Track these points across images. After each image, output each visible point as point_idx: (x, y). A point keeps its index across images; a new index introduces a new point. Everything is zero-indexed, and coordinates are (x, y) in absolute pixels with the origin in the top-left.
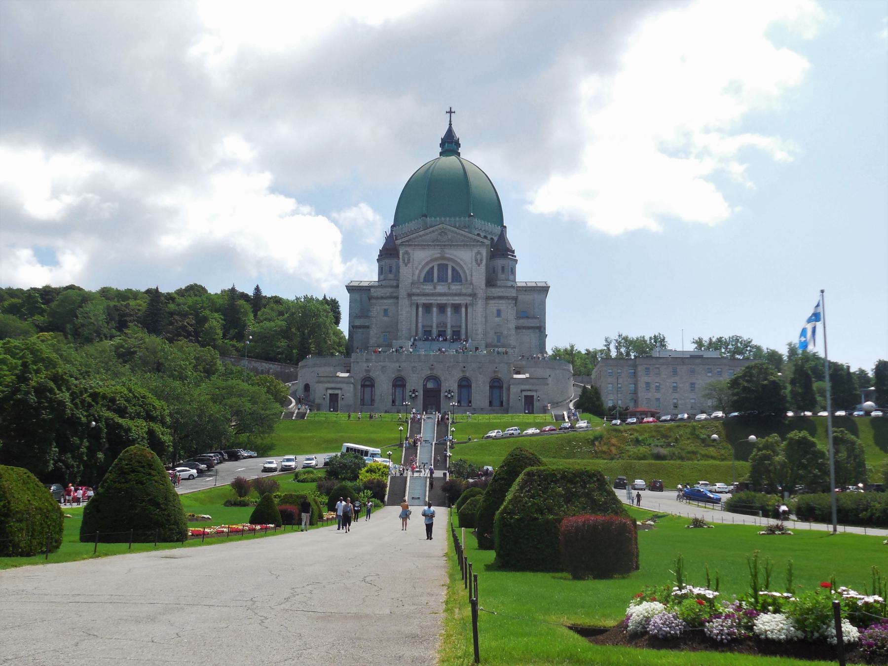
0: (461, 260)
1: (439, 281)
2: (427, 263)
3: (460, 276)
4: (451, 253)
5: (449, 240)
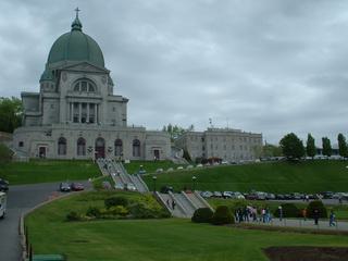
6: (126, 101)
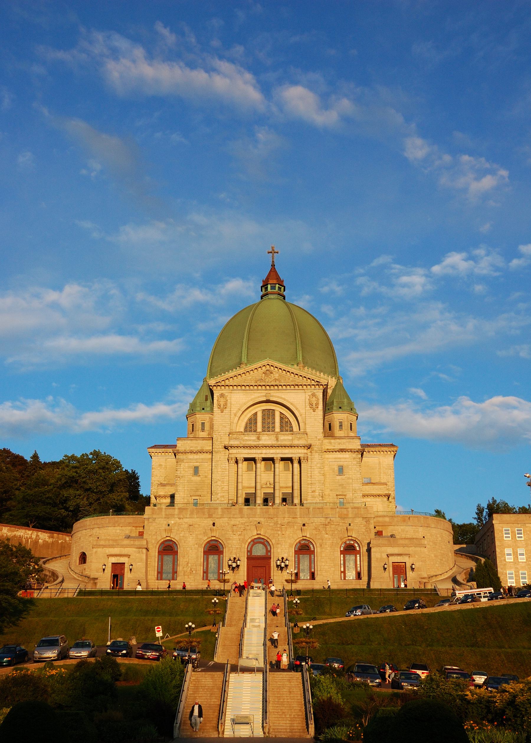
0: (292, 404)
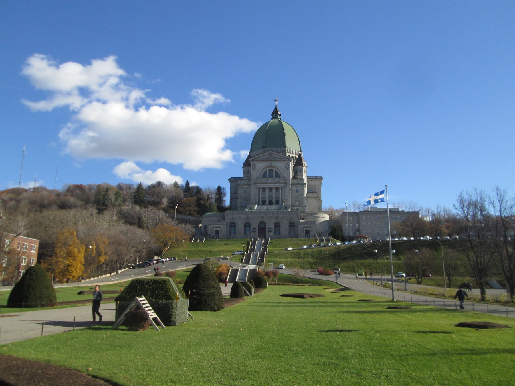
1: (269, 177)
2: (263, 169)
3: (279, 175)
4: (275, 164)
5: (273, 158)
6: (320, 179)
